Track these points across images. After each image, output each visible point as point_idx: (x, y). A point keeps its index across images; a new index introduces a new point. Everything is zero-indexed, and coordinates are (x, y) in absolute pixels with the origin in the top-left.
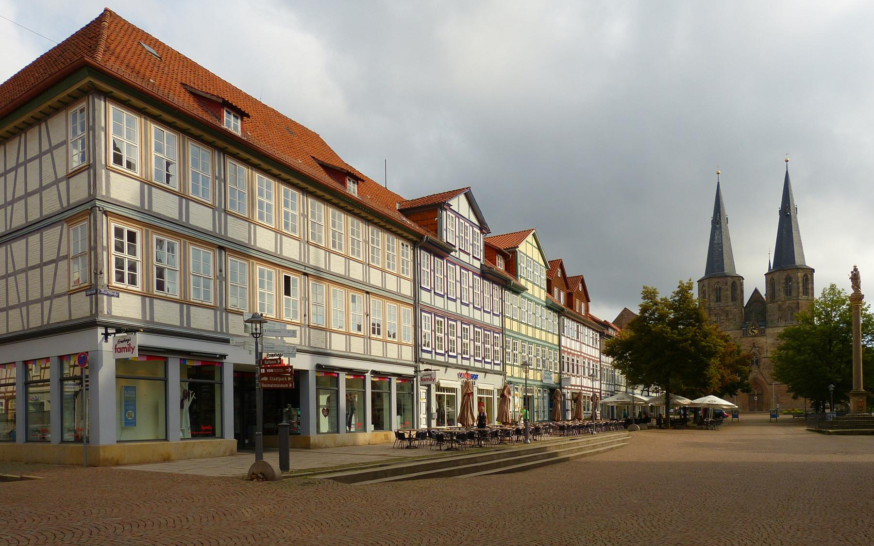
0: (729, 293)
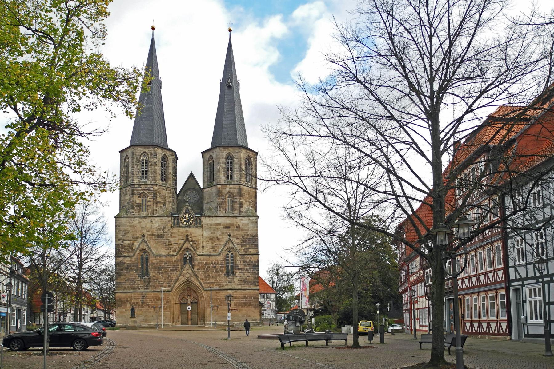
0: (158, 168)
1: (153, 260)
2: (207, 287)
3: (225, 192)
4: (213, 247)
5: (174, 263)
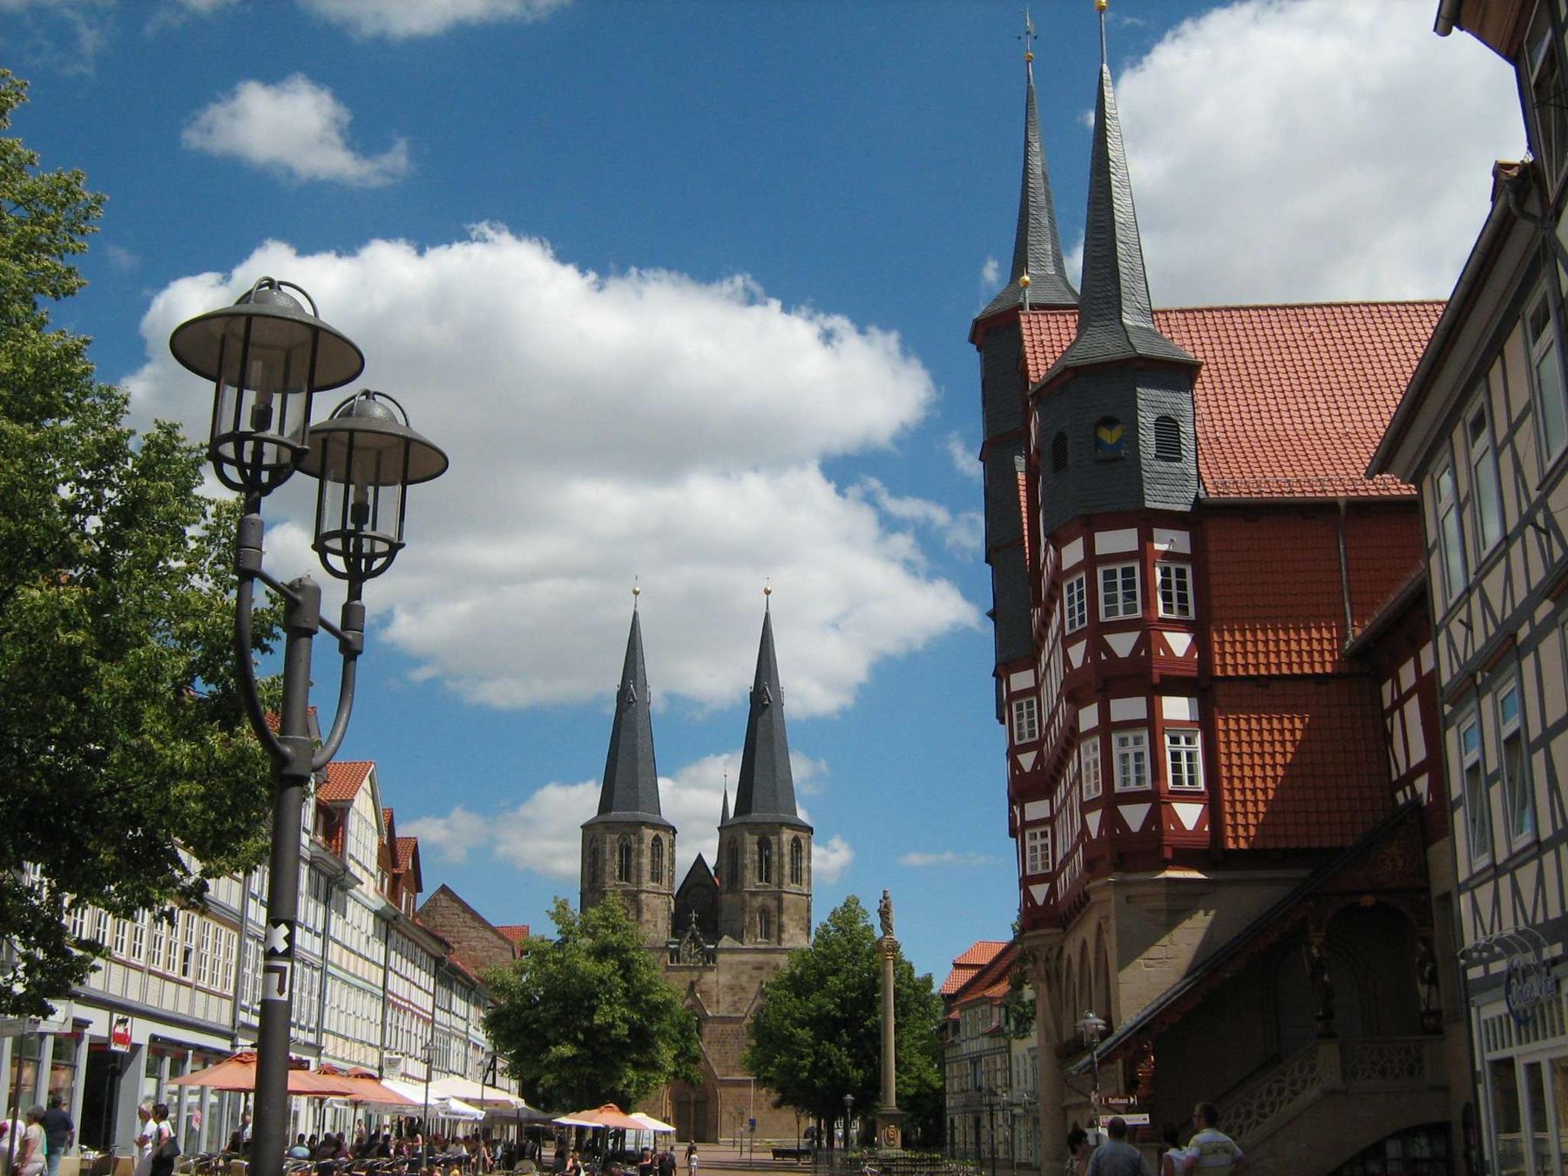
0: (646, 861)
4: (734, 1004)
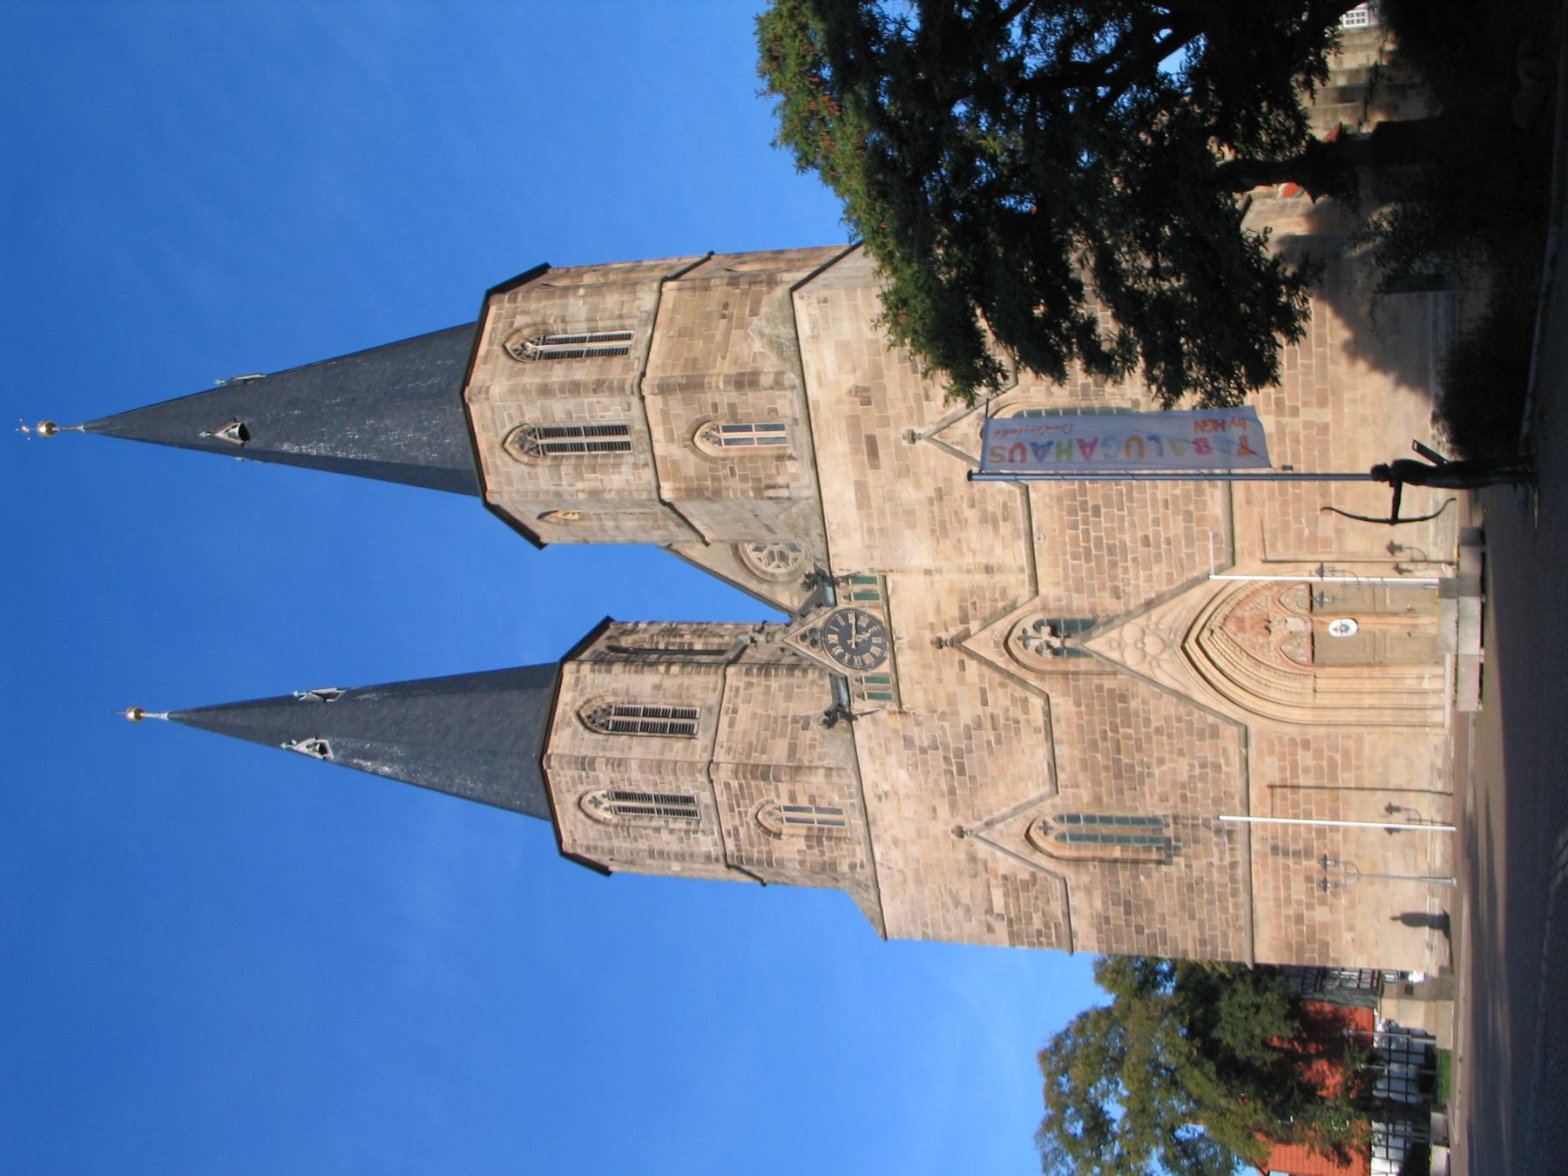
1: (1076, 798)
2: (1217, 551)
3: (691, 466)
4: (989, 520)
5: (1090, 707)
